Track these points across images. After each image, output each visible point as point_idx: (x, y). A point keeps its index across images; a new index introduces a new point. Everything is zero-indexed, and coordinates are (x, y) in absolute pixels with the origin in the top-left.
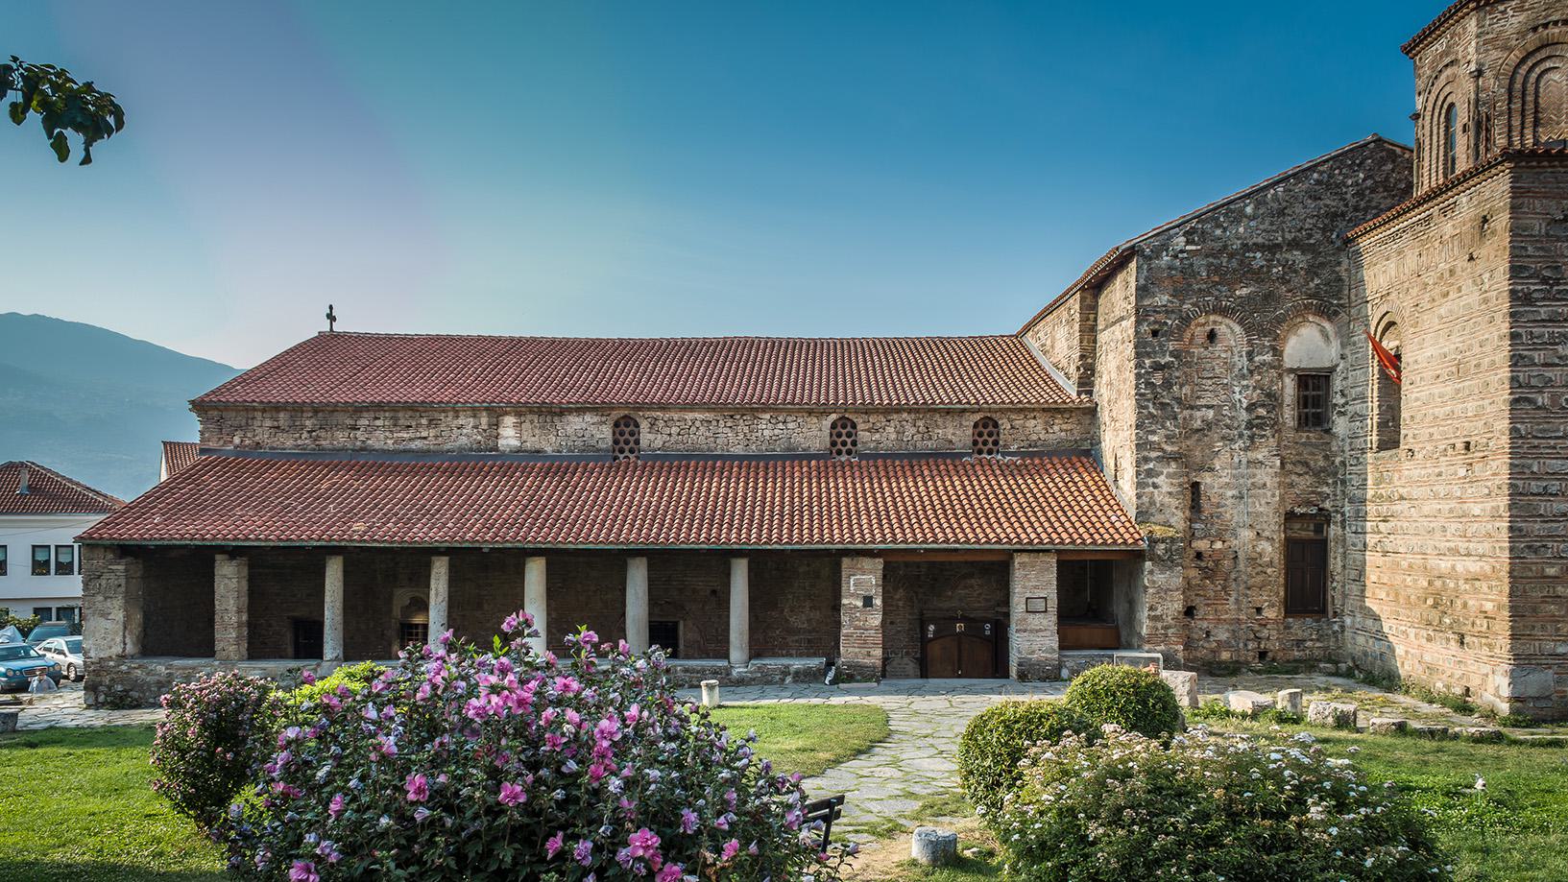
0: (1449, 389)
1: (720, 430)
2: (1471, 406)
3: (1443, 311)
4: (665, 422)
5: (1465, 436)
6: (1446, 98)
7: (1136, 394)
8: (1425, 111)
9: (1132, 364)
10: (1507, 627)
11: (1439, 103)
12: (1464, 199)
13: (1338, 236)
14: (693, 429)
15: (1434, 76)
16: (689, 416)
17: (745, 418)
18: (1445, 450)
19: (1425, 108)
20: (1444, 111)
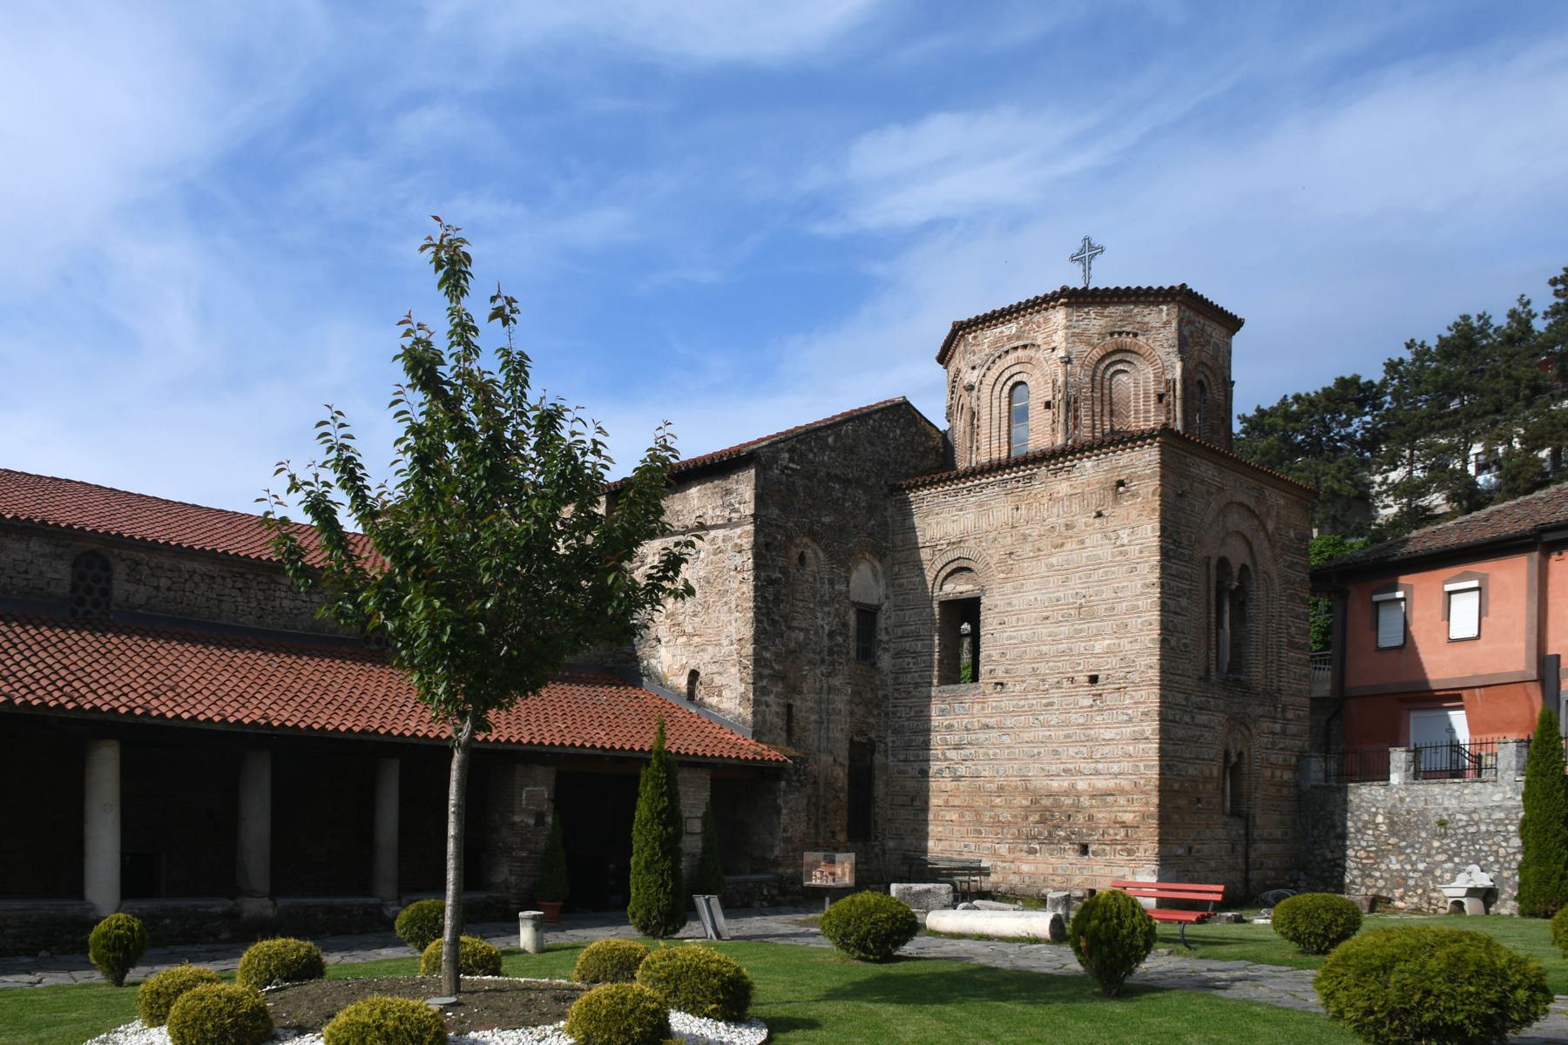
0: (1065, 629)
1: (227, 591)
2: (1100, 646)
3: (1054, 560)
4: (151, 569)
5: (1091, 670)
6: (1012, 376)
7: (755, 607)
8: (981, 383)
9: (749, 576)
10: (1156, 833)
11: (1003, 379)
12: (1088, 464)
13: (885, 482)
14: (190, 584)
15: (996, 355)
16: (187, 565)
17: (259, 579)
18: (1058, 682)
19: (981, 383)
20: (1007, 388)
